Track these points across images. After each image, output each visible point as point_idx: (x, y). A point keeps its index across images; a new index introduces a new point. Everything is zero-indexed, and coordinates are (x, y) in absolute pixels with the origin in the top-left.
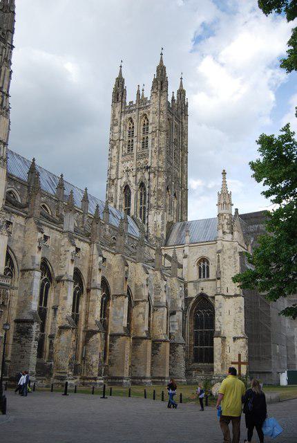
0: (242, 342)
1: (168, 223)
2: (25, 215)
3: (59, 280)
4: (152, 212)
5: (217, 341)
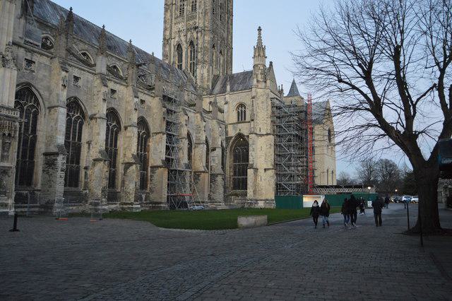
0: (271, 173)
1: (214, 76)
2: (50, 55)
3: (92, 118)
4: (199, 66)
5: (250, 172)
